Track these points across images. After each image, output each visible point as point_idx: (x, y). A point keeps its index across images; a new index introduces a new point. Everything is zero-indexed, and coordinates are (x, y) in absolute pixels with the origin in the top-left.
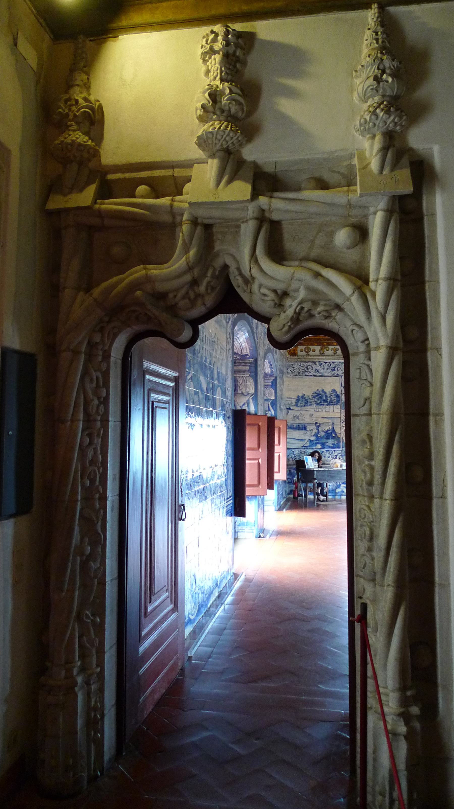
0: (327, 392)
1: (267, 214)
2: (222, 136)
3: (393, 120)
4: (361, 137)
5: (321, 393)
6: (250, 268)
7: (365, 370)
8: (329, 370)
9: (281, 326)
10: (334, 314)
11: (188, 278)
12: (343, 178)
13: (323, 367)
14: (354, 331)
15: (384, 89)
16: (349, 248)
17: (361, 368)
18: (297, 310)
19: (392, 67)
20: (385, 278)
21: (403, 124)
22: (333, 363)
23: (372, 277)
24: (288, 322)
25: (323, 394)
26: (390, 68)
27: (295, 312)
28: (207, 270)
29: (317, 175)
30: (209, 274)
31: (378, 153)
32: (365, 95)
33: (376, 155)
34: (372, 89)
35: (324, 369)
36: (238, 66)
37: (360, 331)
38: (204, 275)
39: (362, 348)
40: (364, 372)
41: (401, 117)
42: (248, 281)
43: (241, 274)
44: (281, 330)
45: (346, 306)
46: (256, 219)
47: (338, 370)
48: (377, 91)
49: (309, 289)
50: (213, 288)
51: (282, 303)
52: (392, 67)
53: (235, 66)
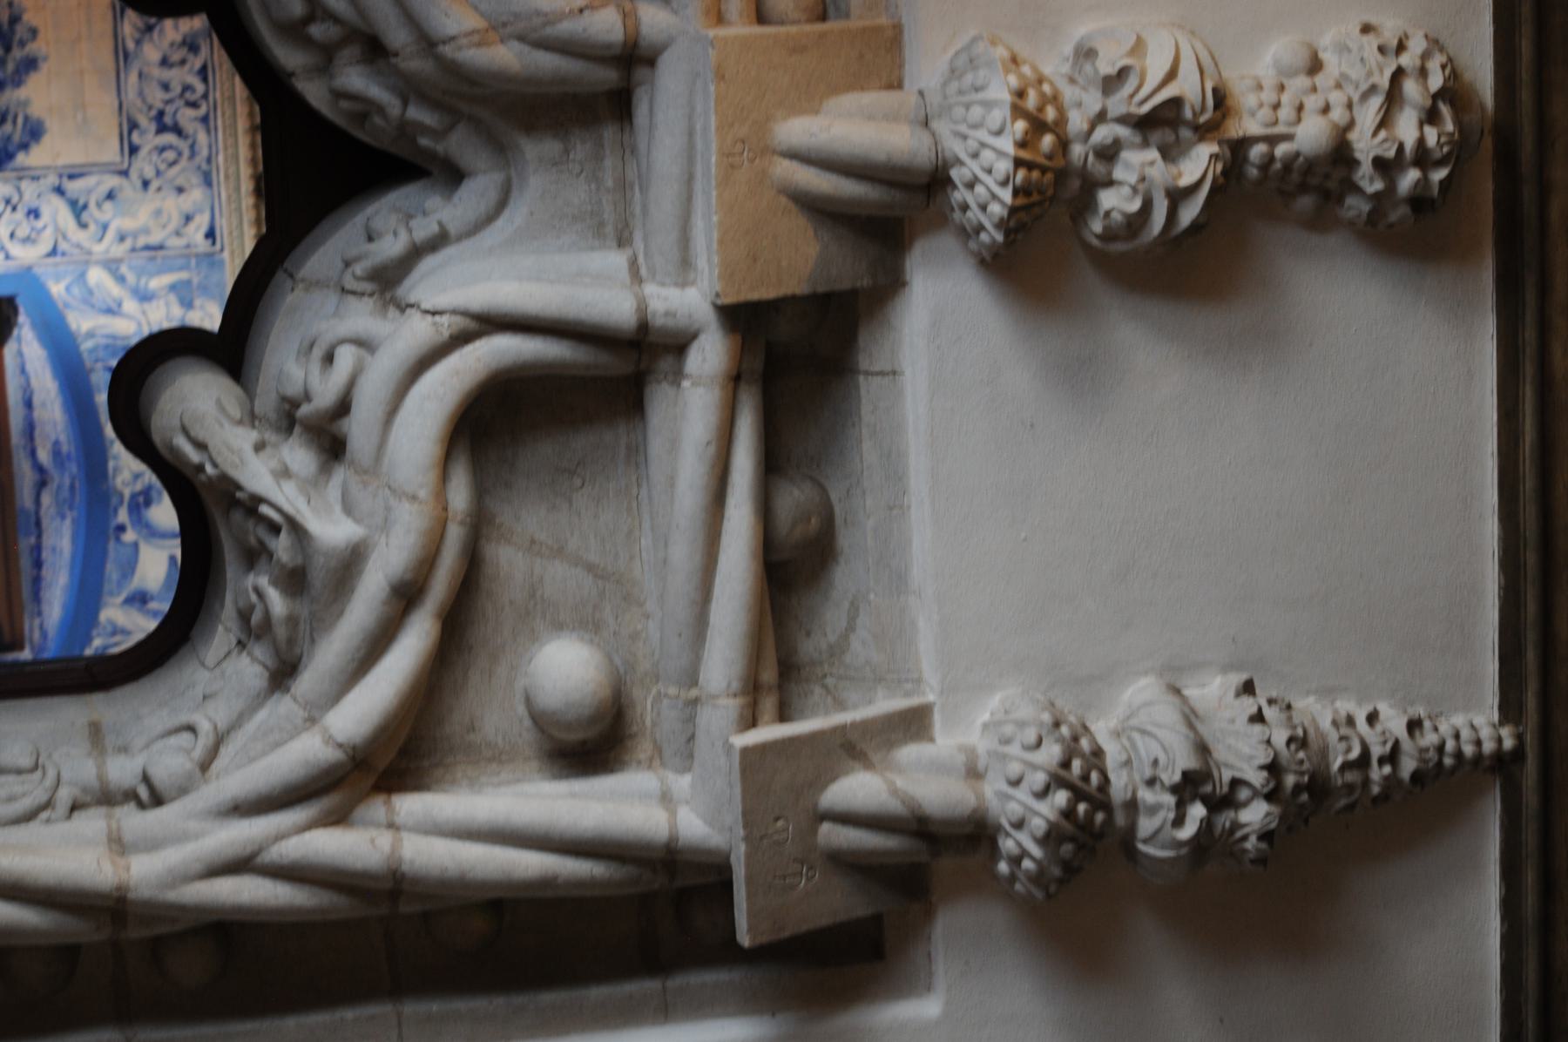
0: (22, 93)
1: (666, 364)
2: (989, 171)
3: (1024, 853)
4: (986, 717)
5: (17, 54)
6: (434, 313)
7: (31, 792)
8: (157, 97)
9: (200, 434)
10: (260, 650)
11: (397, 36)
12: (831, 647)
13: (176, 57)
14: (186, 737)
15: (1153, 810)
16: (528, 701)
17: (39, 773)
18: (265, 509)
19: (1239, 834)
20: (400, 860)
21: (1018, 887)
22: (205, 120)
23: (410, 805)
24: (215, 465)
25: (10, 67)
26: (1236, 825)
27: (258, 500)
28: (435, 104)
29: (844, 540)
30: (416, 113)
31: (907, 800)
32: (1143, 732)
33: (894, 792)
34: (1155, 762)
35: (165, 62)
36: (1306, 202)
37: (188, 766)
38: (410, 89)
39: (122, 771)
40: (18, 789)
41: (1038, 878)
42: (387, 282)
43: (416, 253)
44: (185, 431)
45: (284, 707)
46: (644, 327)
47: (162, 150)
48: (1151, 782)
49: (351, 561)
50: (362, 118)
51: (297, 429)
52: (1239, 834)
53: (1303, 188)
